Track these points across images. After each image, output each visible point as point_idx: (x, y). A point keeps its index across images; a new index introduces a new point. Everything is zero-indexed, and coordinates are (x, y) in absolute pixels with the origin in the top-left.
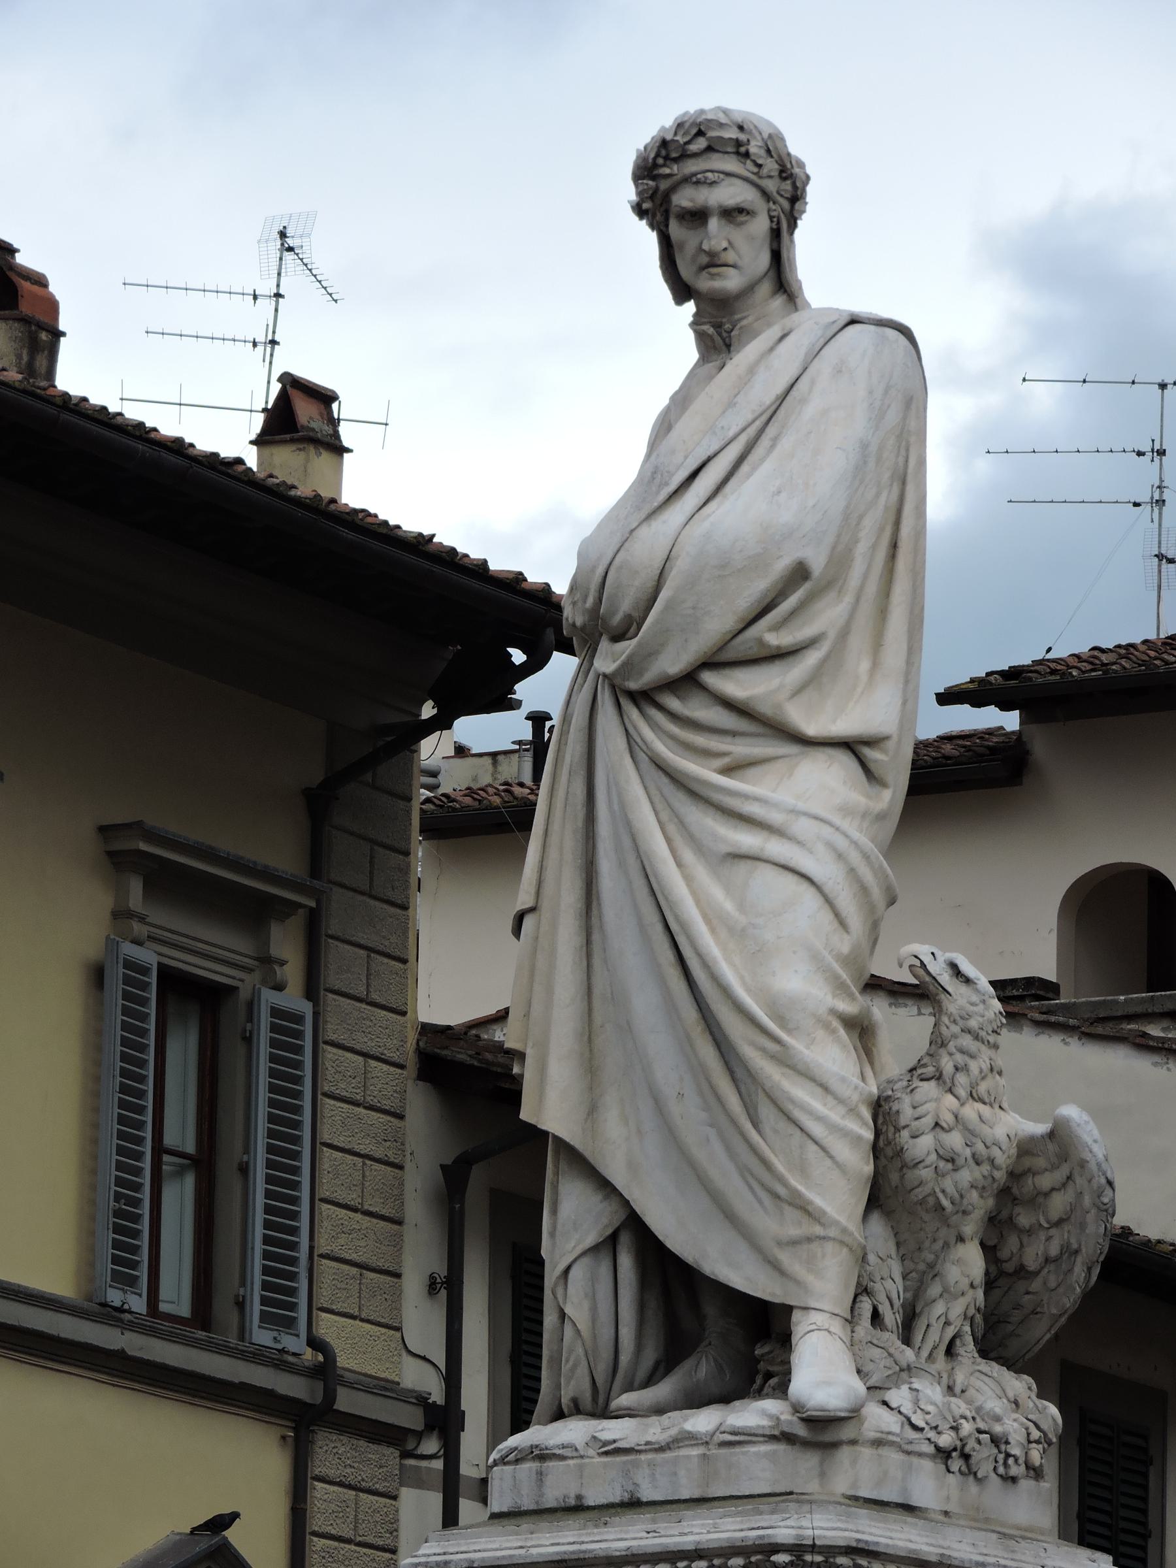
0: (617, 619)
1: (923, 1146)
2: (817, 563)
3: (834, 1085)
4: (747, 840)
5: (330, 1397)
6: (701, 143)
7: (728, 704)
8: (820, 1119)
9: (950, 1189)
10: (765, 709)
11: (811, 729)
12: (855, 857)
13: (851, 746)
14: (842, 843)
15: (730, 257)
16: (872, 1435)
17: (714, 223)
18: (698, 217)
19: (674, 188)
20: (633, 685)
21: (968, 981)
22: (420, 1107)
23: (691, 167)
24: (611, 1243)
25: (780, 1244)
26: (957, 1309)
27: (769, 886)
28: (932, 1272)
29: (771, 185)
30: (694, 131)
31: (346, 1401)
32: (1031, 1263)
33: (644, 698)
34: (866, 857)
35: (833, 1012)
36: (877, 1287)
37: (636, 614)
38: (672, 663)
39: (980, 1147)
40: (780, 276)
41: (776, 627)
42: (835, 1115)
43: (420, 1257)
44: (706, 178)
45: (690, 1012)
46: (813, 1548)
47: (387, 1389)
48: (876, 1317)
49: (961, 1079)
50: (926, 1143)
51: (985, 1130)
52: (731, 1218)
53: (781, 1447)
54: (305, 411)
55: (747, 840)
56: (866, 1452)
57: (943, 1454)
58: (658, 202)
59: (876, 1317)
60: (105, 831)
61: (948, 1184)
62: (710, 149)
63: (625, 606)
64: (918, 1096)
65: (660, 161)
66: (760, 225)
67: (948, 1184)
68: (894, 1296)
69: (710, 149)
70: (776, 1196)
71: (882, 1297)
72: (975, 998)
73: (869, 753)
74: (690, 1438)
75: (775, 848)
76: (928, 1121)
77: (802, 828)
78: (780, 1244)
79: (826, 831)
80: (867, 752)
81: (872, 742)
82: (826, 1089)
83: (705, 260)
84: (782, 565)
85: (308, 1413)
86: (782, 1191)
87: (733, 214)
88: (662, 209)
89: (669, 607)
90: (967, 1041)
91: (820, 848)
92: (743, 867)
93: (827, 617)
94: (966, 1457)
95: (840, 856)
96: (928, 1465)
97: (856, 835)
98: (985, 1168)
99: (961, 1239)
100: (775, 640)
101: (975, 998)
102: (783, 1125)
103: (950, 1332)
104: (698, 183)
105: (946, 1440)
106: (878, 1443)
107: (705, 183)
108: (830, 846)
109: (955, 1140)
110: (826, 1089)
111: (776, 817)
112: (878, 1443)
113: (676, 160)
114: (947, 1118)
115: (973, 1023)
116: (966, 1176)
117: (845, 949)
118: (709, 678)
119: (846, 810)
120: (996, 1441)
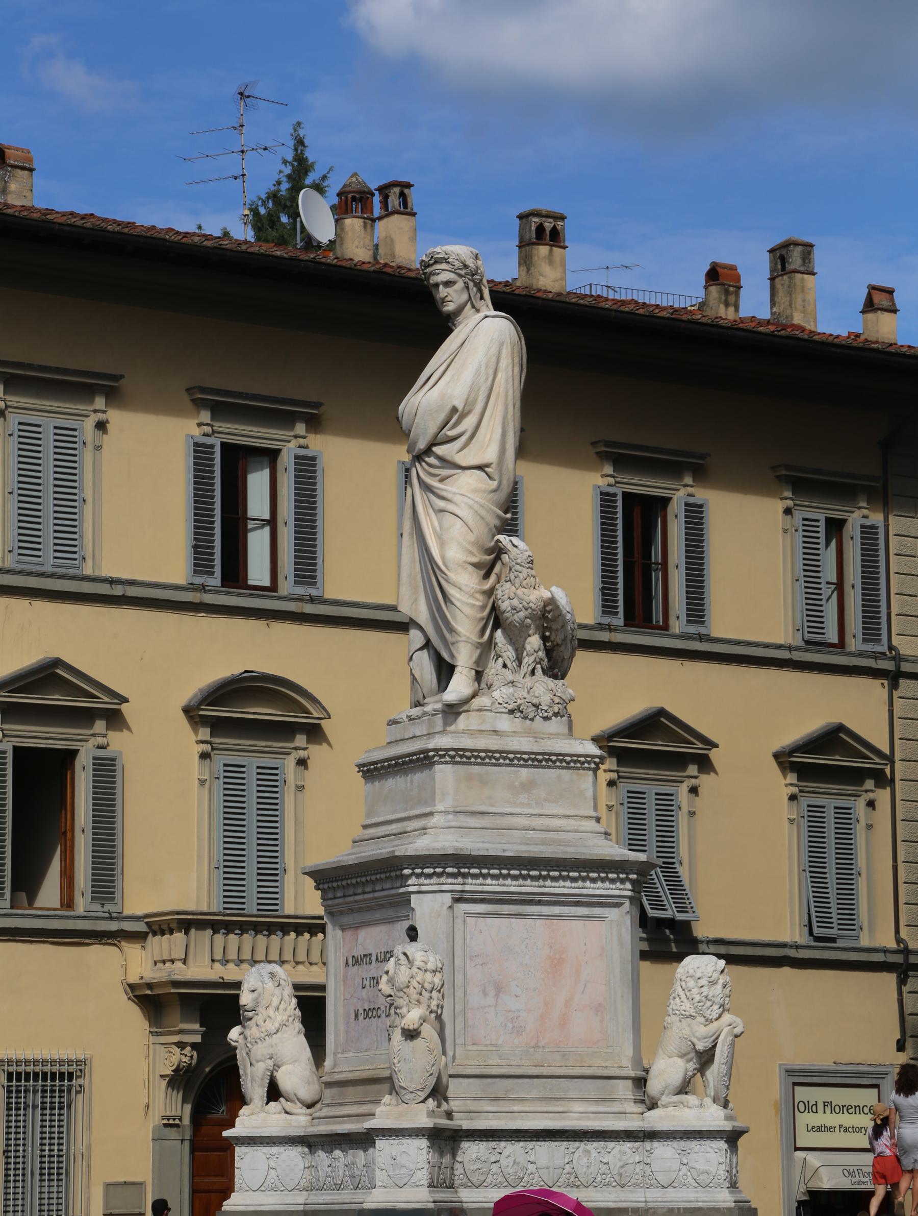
1: (505, 605)
2: (460, 407)
3: (464, 588)
5: (898, 667)
7: (440, 458)
8: (458, 600)
9: (517, 619)
10: (448, 458)
11: (464, 464)
12: (477, 507)
13: (480, 468)
14: (471, 502)
15: (449, 298)
16: (476, 708)
17: (441, 287)
18: (437, 285)
21: (516, 547)
26: (532, 659)
27: (448, 518)
28: (524, 648)
29: (463, 272)
31: (905, 667)
32: (560, 642)
34: (482, 506)
35: (465, 562)
36: (504, 654)
39: (525, 603)
42: (465, 598)
46: (441, 750)
48: (505, 666)
49: (517, 580)
50: (507, 603)
51: (526, 598)
54: (879, 298)
56: (475, 713)
57: (511, 712)
59: (505, 666)
61: (516, 617)
62: (436, 262)
64: (504, 588)
66: (460, 284)
67: (516, 617)
68: (511, 657)
71: (506, 658)
72: (519, 552)
73: (486, 469)
76: (506, 597)
77: (457, 499)
79: (465, 499)
80: (486, 469)
81: (488, 466)
82: (460, 589)
84: (448, 408)
87: (448, 284)
90: (517, 567)
91: (463, 505)
93: (468, 423)
94: (522, 712)
95: (471, 507)
96: (507, 715)
97: (477, 499)
98: (530, 611)
99: (530, 636)
100: (451, 433)
101: (519, 552)
103: (531, 668)
105: (510, 707)
106: (480, 710)
108: (466, 503)
109: (515, 602)
110: (460, 589)
111: (449, 496)
112: (480, 710)
114: (512, 595)
115: (519, 561)
116: (522, 614)
117: (472, 540)
119: (476, 491)
120: (534, 705)
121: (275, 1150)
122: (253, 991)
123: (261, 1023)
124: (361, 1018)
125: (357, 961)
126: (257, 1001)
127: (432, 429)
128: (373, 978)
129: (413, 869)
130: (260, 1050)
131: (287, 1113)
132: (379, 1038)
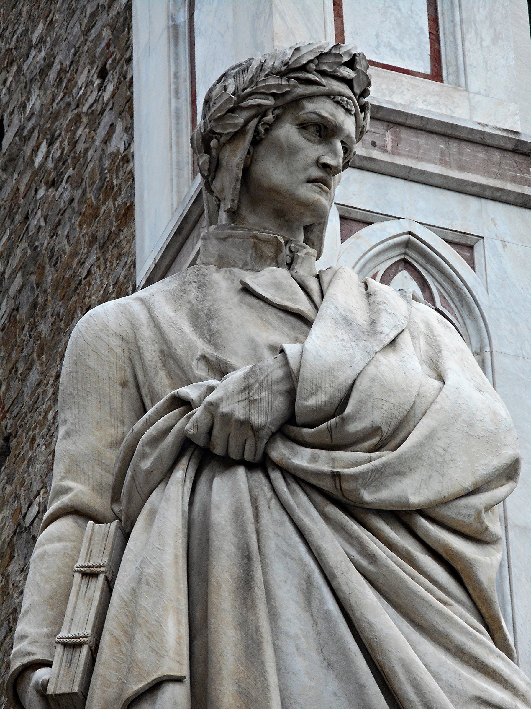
0: (354, 427)
6: (347, 72)
18: (325, 131)
19: (310, 97)
30: (346, 59)
37: (386, 430)
44: (348, 103)
58: (280, 102)
62: (349, 83)
65: (313, 66)
69: (349, 83)
83: (316, 173)
88: (277, 112)
89: (431, 436)
104: (338, 103)
107: (343, 107)
113: (324, 74)
127: (461, 477)
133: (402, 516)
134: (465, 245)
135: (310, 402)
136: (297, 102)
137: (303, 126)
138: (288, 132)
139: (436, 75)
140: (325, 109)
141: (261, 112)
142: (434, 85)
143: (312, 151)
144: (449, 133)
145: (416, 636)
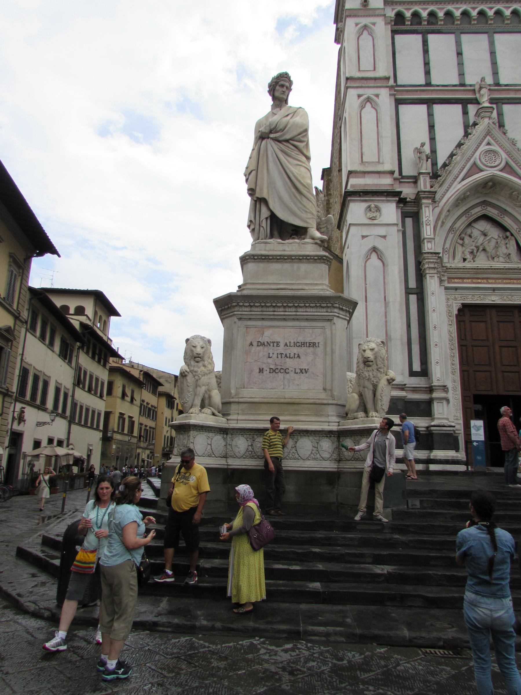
0: (278, 129)
4: (299, 163)
18: (282, 86)
20: (281, 139)
22: (28, 292)
23: (284, 79)
24: (267, 218)
25: (307, 218)
31: (20, 318)
33: (279, 141)
38: (287, 137)
40: (286, 101)
41: (302, 137)
43: (26, 306)
45: (290, 184)
47: (23, 317)
52: (294, 214)
53: (314, 245)
55: (299, 163)
60: (10, 253)
62: (286, 77)
63: (281, 127)
69: (286, 77)
70: (307, 212)
74: (296, 242)
75: (303, 165)
78: (307, 218)
84: (304, 128)
85: (17, 317)
86: (307, 210)
87: (287, 88)
89: (290, 128)
92: (298, 167)
100: (301, 138)
102: (308, 201)
118: (291, 142)
121: (211, 435)
122: (202, 348)
123: (207, 365)
124: (266, 372)
125: (261, 344)
126: (204, 353)
128: (282, 354)
129: (339, 305)
130: (204, 380)
131: (214, 414)
132: (286, 383)
133: (287, 141)
134: (377, 96)
135: (272, 127)
136: (278, 83)
137: (280, 86)
138: (278, 87)
139: (375, 70)
140: (282, 83)
141: (274, 85)
142: (374, 72)
143: (281, 89)
144: (375, 79)
145: (287, 157)
